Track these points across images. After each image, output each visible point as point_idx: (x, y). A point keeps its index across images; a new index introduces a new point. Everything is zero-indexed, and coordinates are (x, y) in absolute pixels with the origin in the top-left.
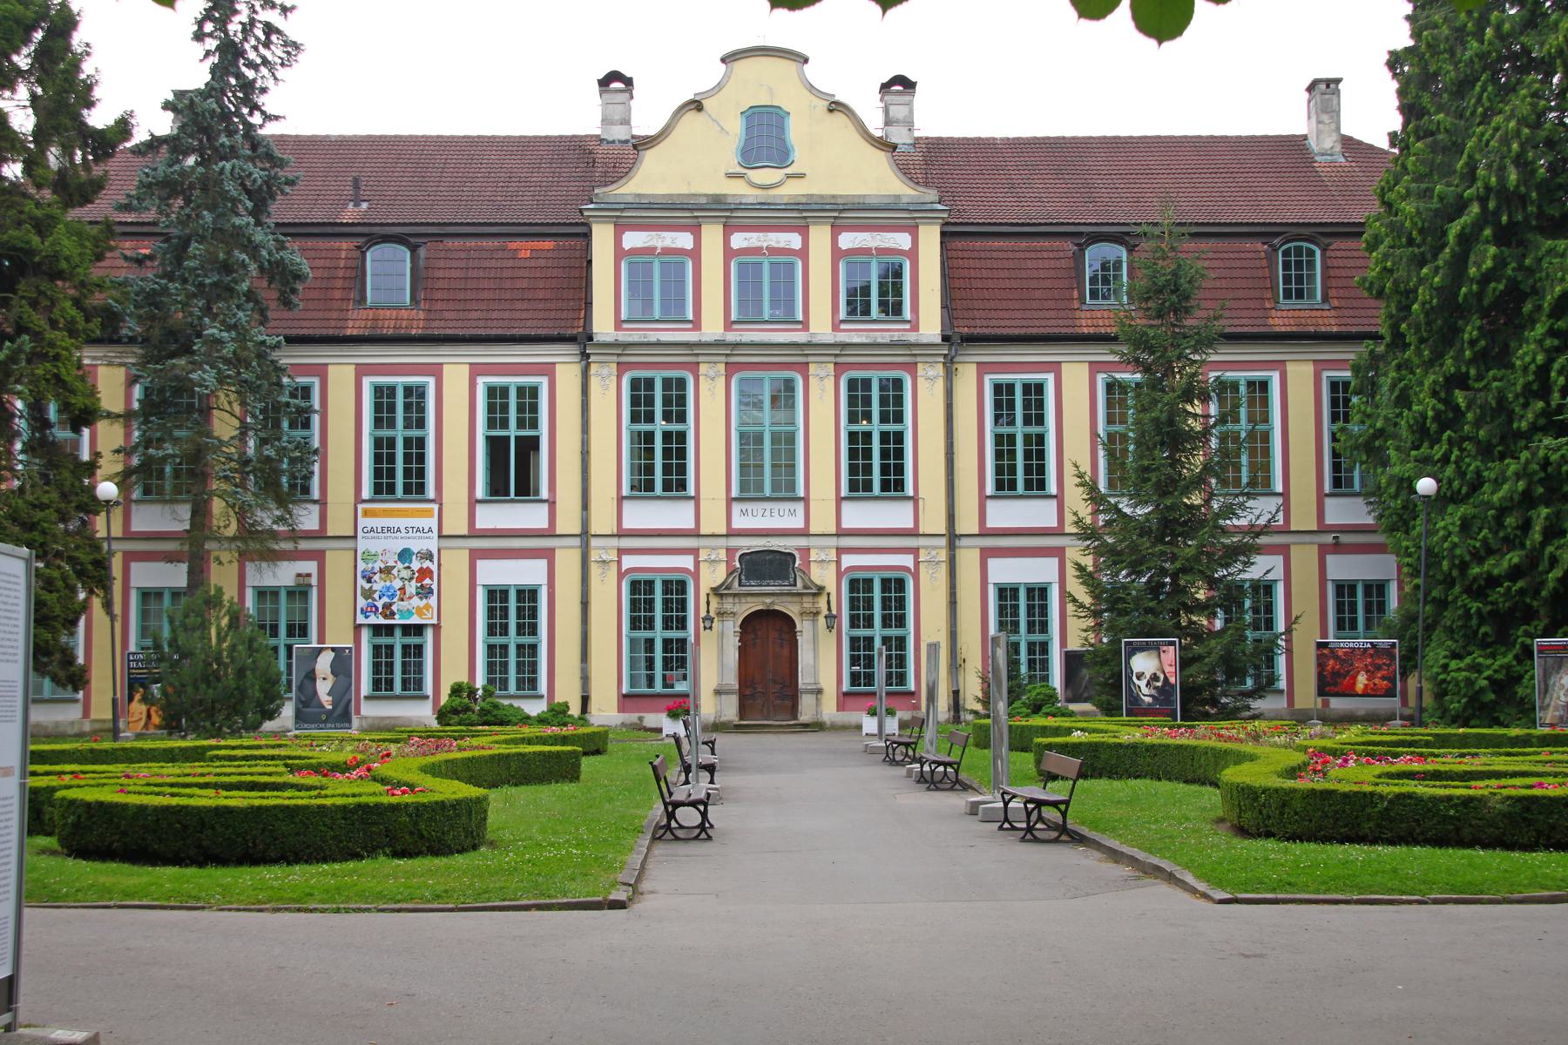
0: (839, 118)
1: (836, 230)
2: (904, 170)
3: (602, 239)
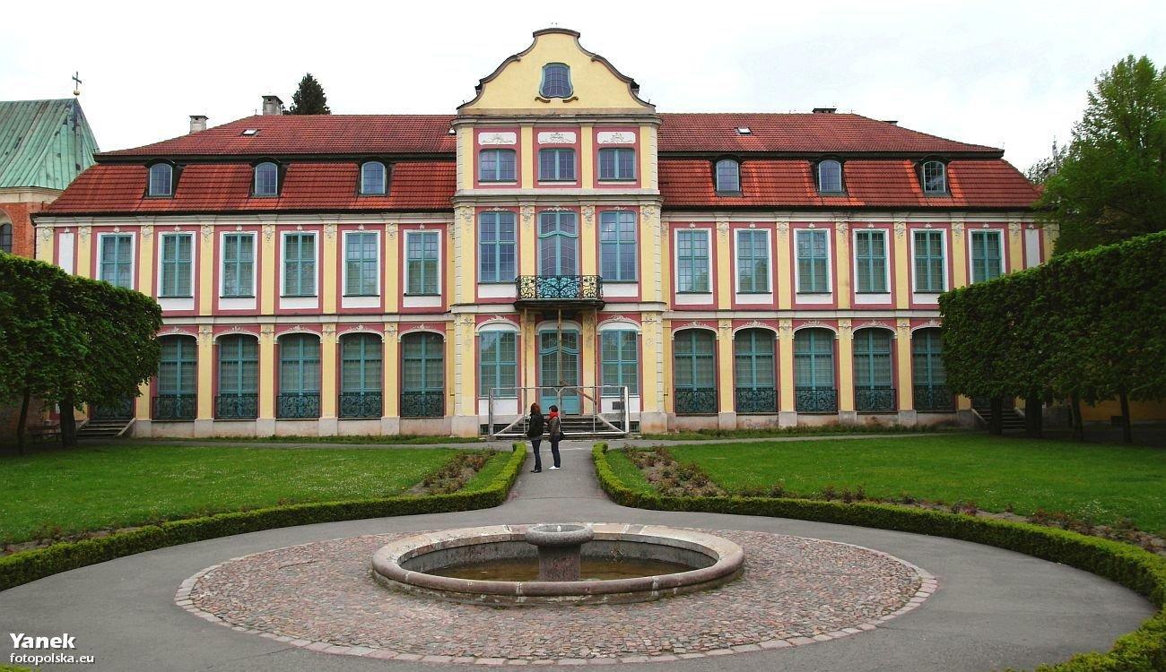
0: (598, 65)
1: (596, 130)
3: (465, 142)
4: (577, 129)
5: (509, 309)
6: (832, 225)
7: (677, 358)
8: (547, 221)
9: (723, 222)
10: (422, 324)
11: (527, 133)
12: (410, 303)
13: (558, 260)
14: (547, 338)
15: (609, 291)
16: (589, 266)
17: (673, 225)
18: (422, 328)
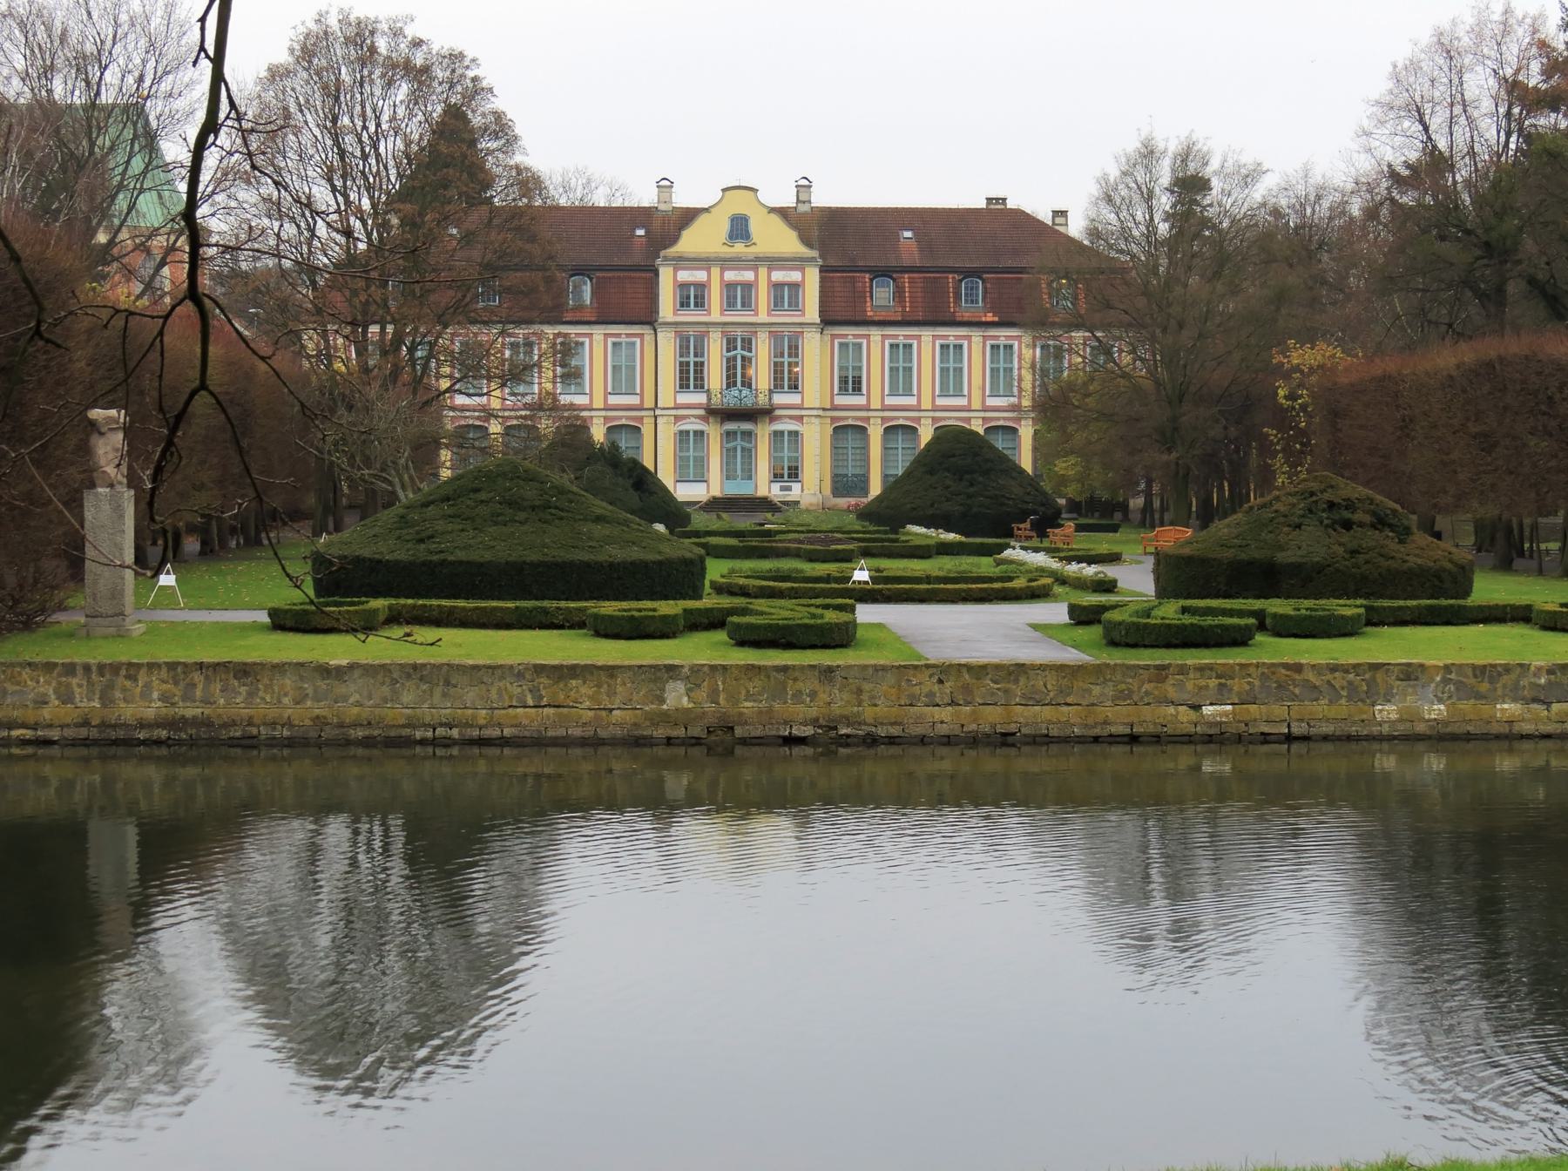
1: (770, 269)
2: (806, 241)
4: (755, 269)
5: (702, 412)
6: (969, 338)
7: (834, 448)
8: (731, 344)
9: (876, 334)
10: (623, 418)
11: (715, 271)
12: (613, 400)
13: (736, 373)
14: (729, 435)
15: (778, 399)
16: (762, 376)
17: (833, 337)
18: (624, 422)
